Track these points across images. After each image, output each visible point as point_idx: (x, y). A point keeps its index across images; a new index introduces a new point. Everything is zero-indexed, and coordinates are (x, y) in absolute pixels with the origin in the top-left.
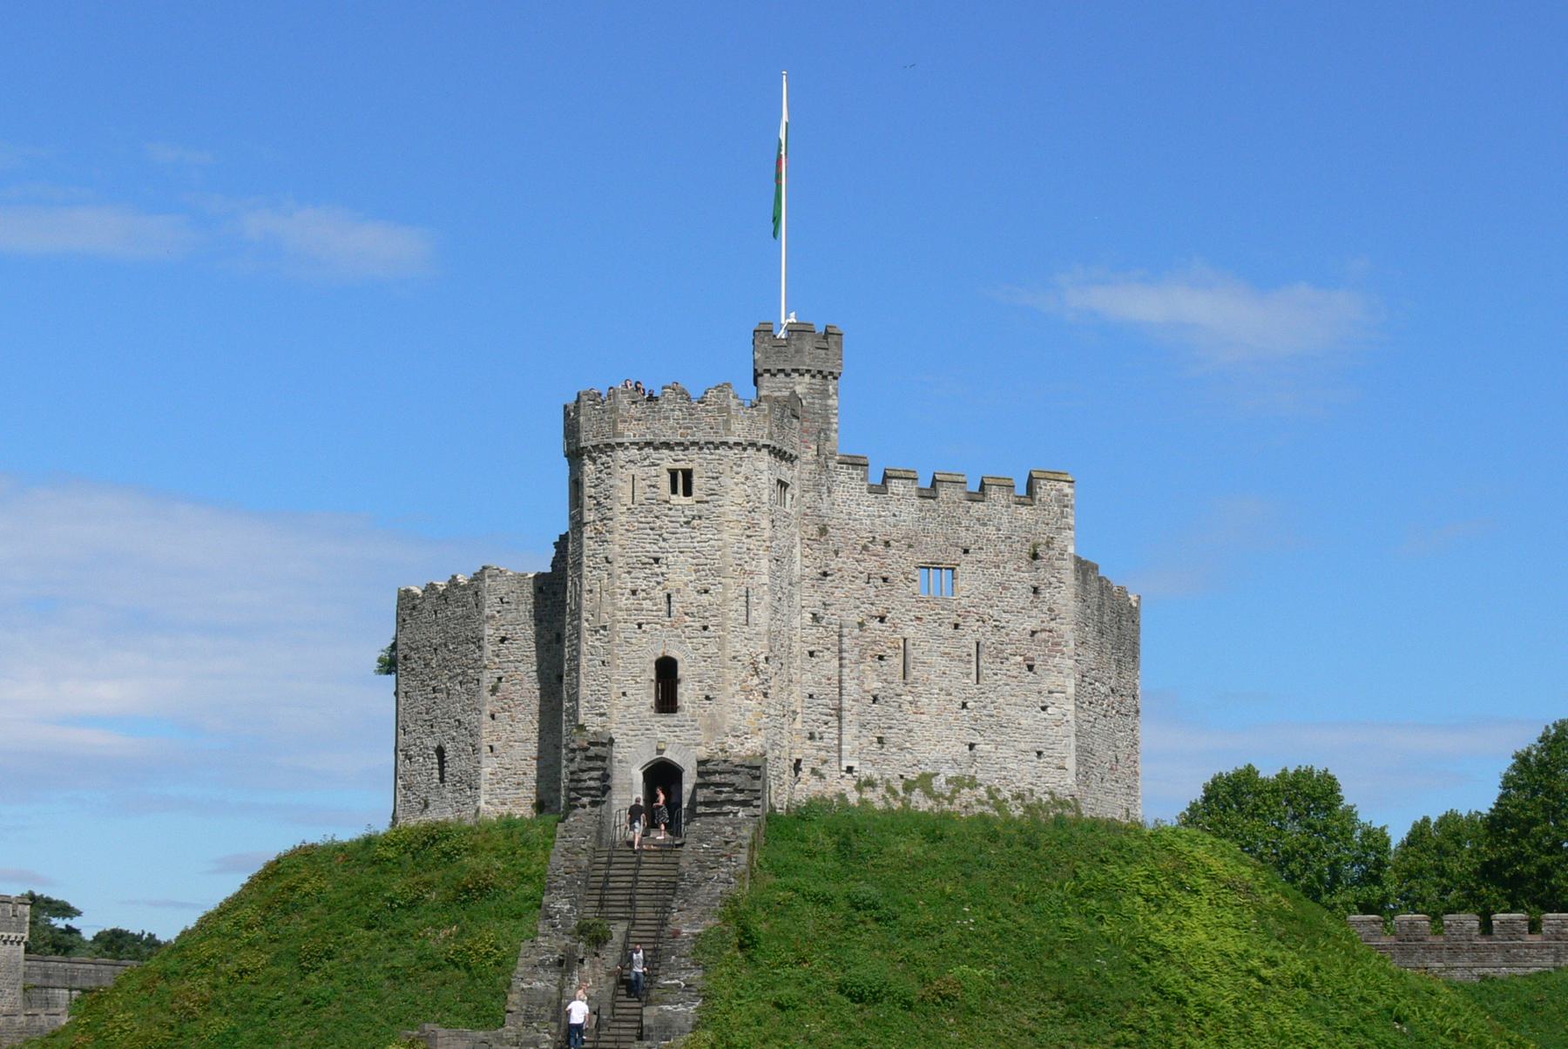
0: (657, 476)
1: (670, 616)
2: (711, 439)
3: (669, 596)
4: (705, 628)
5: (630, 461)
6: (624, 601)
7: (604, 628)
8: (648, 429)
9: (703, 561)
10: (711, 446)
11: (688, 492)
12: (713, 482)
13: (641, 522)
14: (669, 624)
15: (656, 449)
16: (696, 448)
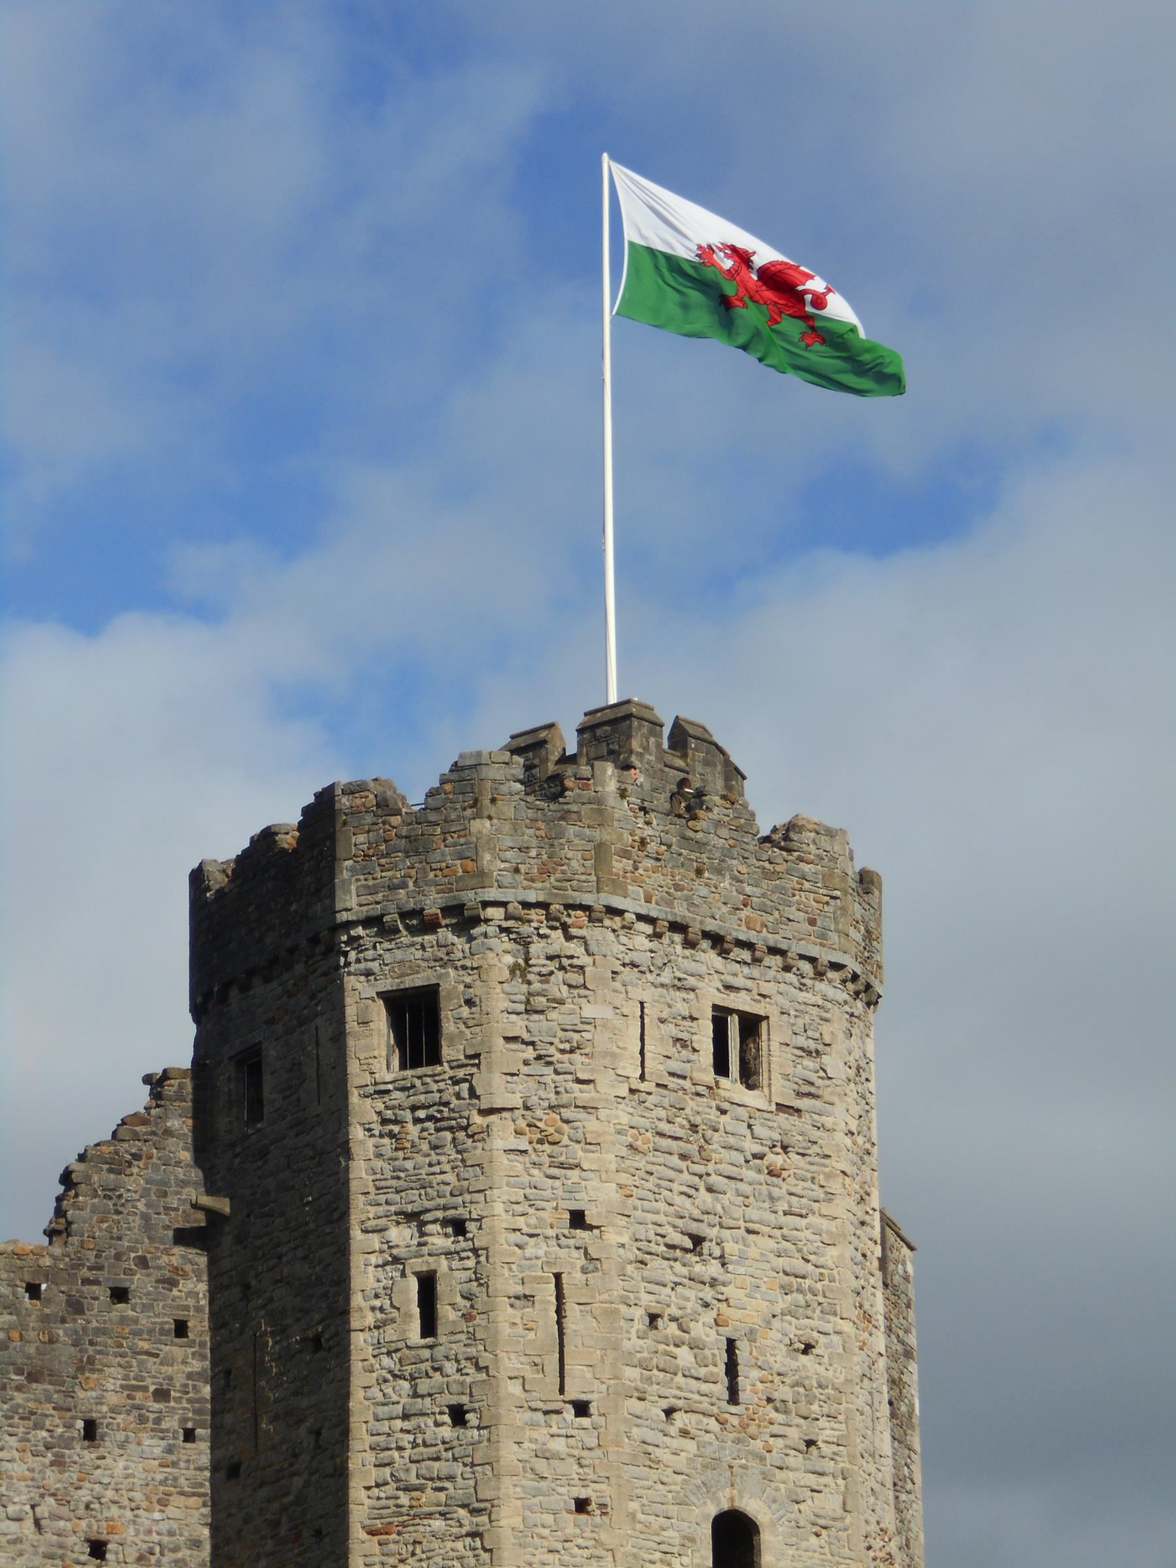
0: (693, 1019)
1: (733, 1396)
2: (814, 951)
3: (731, 1344)
4: (810, 1443)
5: (634, 965)
6: (634, 1340)
7: (582, 1409)
8: (678, 888)
9: (798, 1265)
10: (806, 967)
11: (749, 1077)
12: (808, 1062)
13: (661, 1134)
14: (735, 1421)
15: (690, 944)
16: (777, 960)
